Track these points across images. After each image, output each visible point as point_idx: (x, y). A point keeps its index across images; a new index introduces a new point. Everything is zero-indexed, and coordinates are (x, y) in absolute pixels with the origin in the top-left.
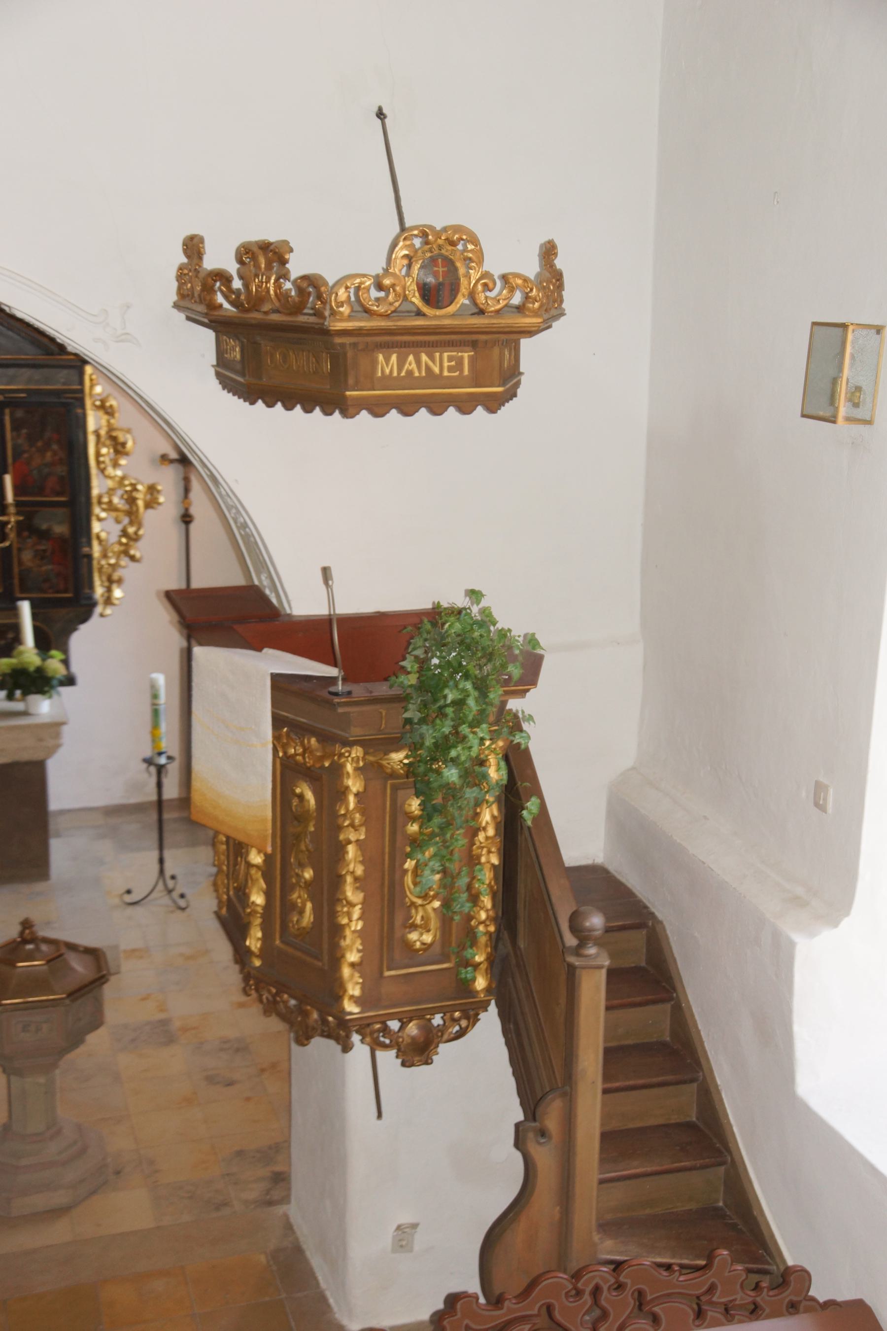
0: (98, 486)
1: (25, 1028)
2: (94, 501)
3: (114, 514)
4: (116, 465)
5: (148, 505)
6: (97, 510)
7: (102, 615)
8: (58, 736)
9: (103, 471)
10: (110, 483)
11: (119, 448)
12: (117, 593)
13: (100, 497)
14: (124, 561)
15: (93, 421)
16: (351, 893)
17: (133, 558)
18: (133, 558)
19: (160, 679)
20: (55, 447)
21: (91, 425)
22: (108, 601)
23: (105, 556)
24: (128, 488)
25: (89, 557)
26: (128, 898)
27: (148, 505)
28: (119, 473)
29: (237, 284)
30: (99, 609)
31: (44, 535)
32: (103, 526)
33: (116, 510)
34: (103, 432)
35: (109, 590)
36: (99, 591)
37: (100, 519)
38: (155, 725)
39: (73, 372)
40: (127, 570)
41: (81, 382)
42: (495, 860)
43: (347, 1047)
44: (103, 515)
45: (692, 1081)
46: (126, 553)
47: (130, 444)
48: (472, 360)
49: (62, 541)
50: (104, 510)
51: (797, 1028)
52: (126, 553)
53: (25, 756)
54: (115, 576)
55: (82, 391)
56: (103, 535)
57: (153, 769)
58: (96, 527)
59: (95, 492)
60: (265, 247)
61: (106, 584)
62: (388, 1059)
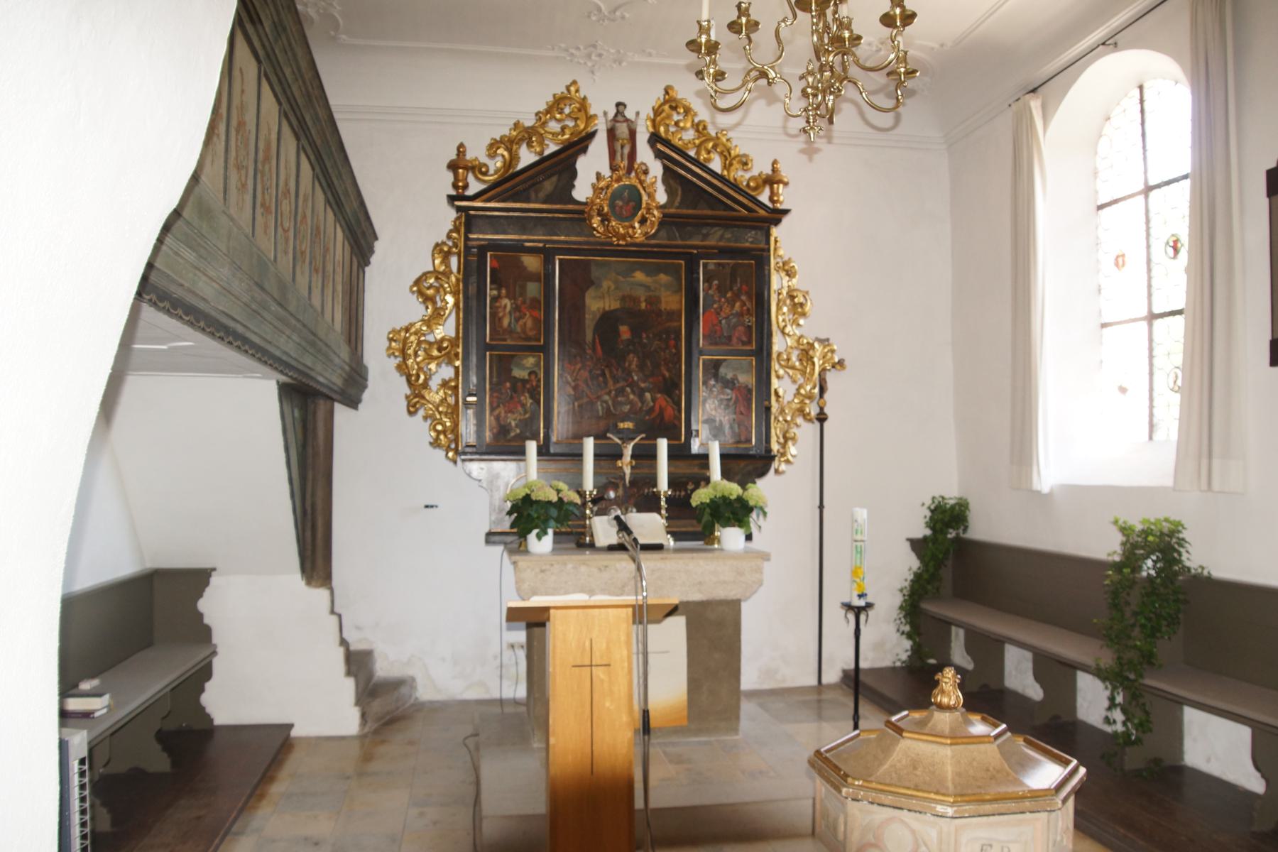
0: (779, 344)
2: (774, 356)
3: (791, 372)
6: (775, 366)
7: (777, 471)
9: (783, 332)
10: (790, 342)
11: (798, 309)
12: (792, 450)
13: (779, 354)
14: (799, 420)
15: (778, 282)
20: (744, 298)
21: (775, 285)
23: (782, 411)
24: (805, 347)
28: (798, 333)
30: (775, 464)
33: (793, 368)
34: (784, 292)
35: (784, 445)
37: (778, 377)
41: (768, 242)
44: (781, 372)
47: (808, 308)
50: (781, 366)
53: (721, 593)
54: (790, 435)
55: (769, 250)
56: (781, 393)
57: (851, 617)
58: (775, 383)
61: (782, 440)
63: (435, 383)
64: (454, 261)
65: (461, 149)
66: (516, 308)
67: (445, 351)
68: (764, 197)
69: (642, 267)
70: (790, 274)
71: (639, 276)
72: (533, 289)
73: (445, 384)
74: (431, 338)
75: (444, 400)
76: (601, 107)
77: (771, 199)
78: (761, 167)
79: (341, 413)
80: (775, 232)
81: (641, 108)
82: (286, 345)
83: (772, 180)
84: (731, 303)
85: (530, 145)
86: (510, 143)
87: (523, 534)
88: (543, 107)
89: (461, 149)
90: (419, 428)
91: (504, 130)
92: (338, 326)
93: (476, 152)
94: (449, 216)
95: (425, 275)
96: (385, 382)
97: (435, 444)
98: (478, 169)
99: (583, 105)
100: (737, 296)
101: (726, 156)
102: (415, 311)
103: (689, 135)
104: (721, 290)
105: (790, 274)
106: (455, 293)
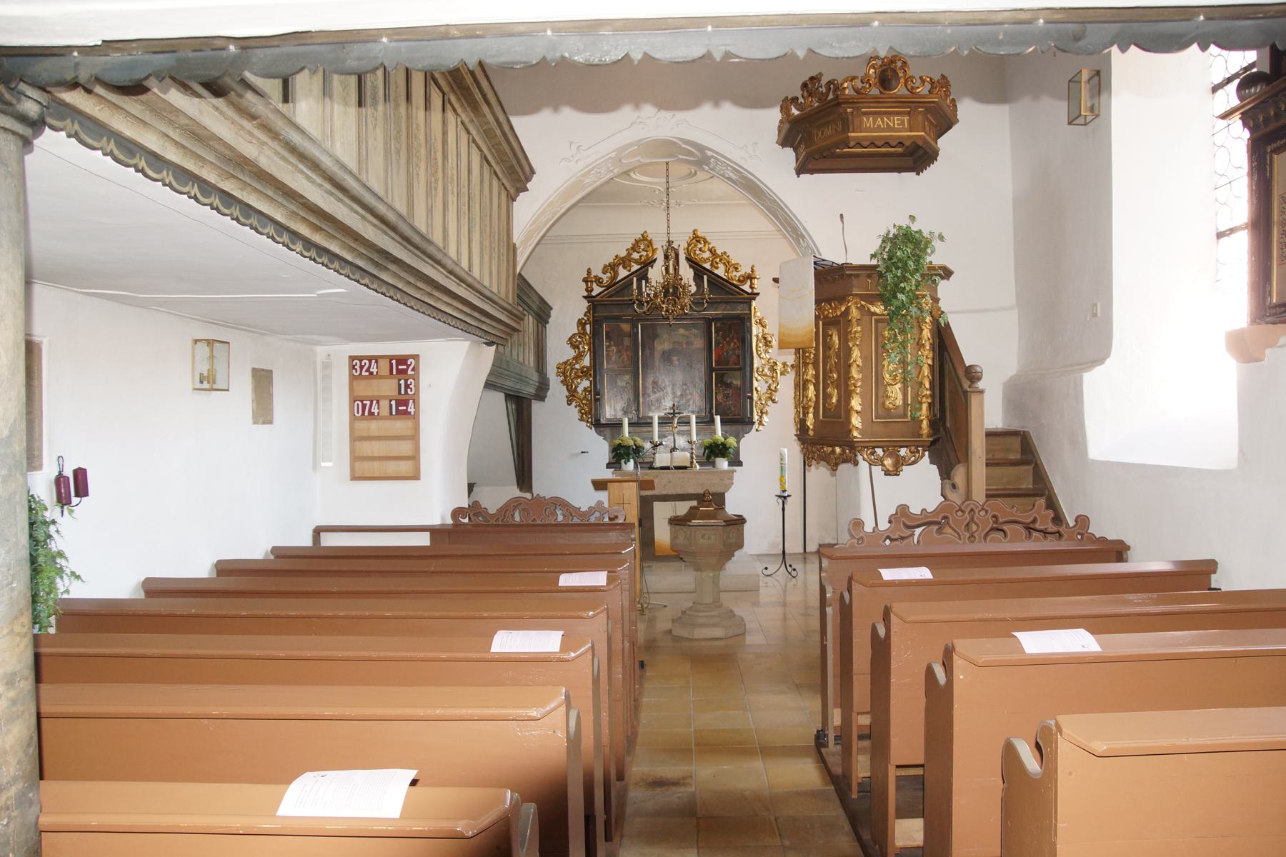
1: (703, 536)
4: (766, 352)
5: (782, 374)
8: (731, 478)
11: (768, 344)
12: (765, 418)
14: (770, 403)
15: (755, 330)
16: (855, 373)
17: (773, 401)
18: (773, 401)
19: (786, 450)
21: (754, 332)
22: (761, 423)
25: (751, 398)
26: (766, 572)
27: (782, 374)
29: (801, 100)
30: (756, 426)
31: (729, 386)
32: (759, 385)
36: (756, 418)
38: (782, 476)
39: (745, 306)
40: (771, 407)
42: (930, 362)
43: (856, 463)
45: (1042, 495)
46: (770, 398)
48: (909, 121)
49: (737, 388)
51: (1087, 422)
52: (770, 398)
58: (755, 384)
59: (755, 366)
60: (812, 78)
62: (877, 470)
63: (580, 389)
64: (588, 327)
65: (589, 271)
66: (619, 351)
67: (584, 373)
68: (746, 287)
69: (684, 326)
70: (764, 326)
71: (682, 331)
72: (627, 341)
73: (585, 389)
74: (577, 366)
75: (585, 398)
76: (659, 244)
77: (751, 287)
78: (744, 270)
79: (536, 406)
80: (754, 304)
81: (681, 243)
82: (509, 384)
83: (750, 277)
84: (729, 343)
85: (624, 267)
86: (612, 267)
87: (618, 462)
88: (630, 246)
89: (589, 271)
90: (573, 411)
91: (610, 260)
92: (532, 364)
93: (597, 271)
94: (585, 304)
95: (574, 335)
96: (557, 390)
97: (581, 419)
98: (599, 281)
99: (650, 243)
100: (732, 340)
101: (728, 265)
102: (570, 353)
103: (707, 255)
104: (724, 337)
105: (764, 326)
106: (589, 344)
